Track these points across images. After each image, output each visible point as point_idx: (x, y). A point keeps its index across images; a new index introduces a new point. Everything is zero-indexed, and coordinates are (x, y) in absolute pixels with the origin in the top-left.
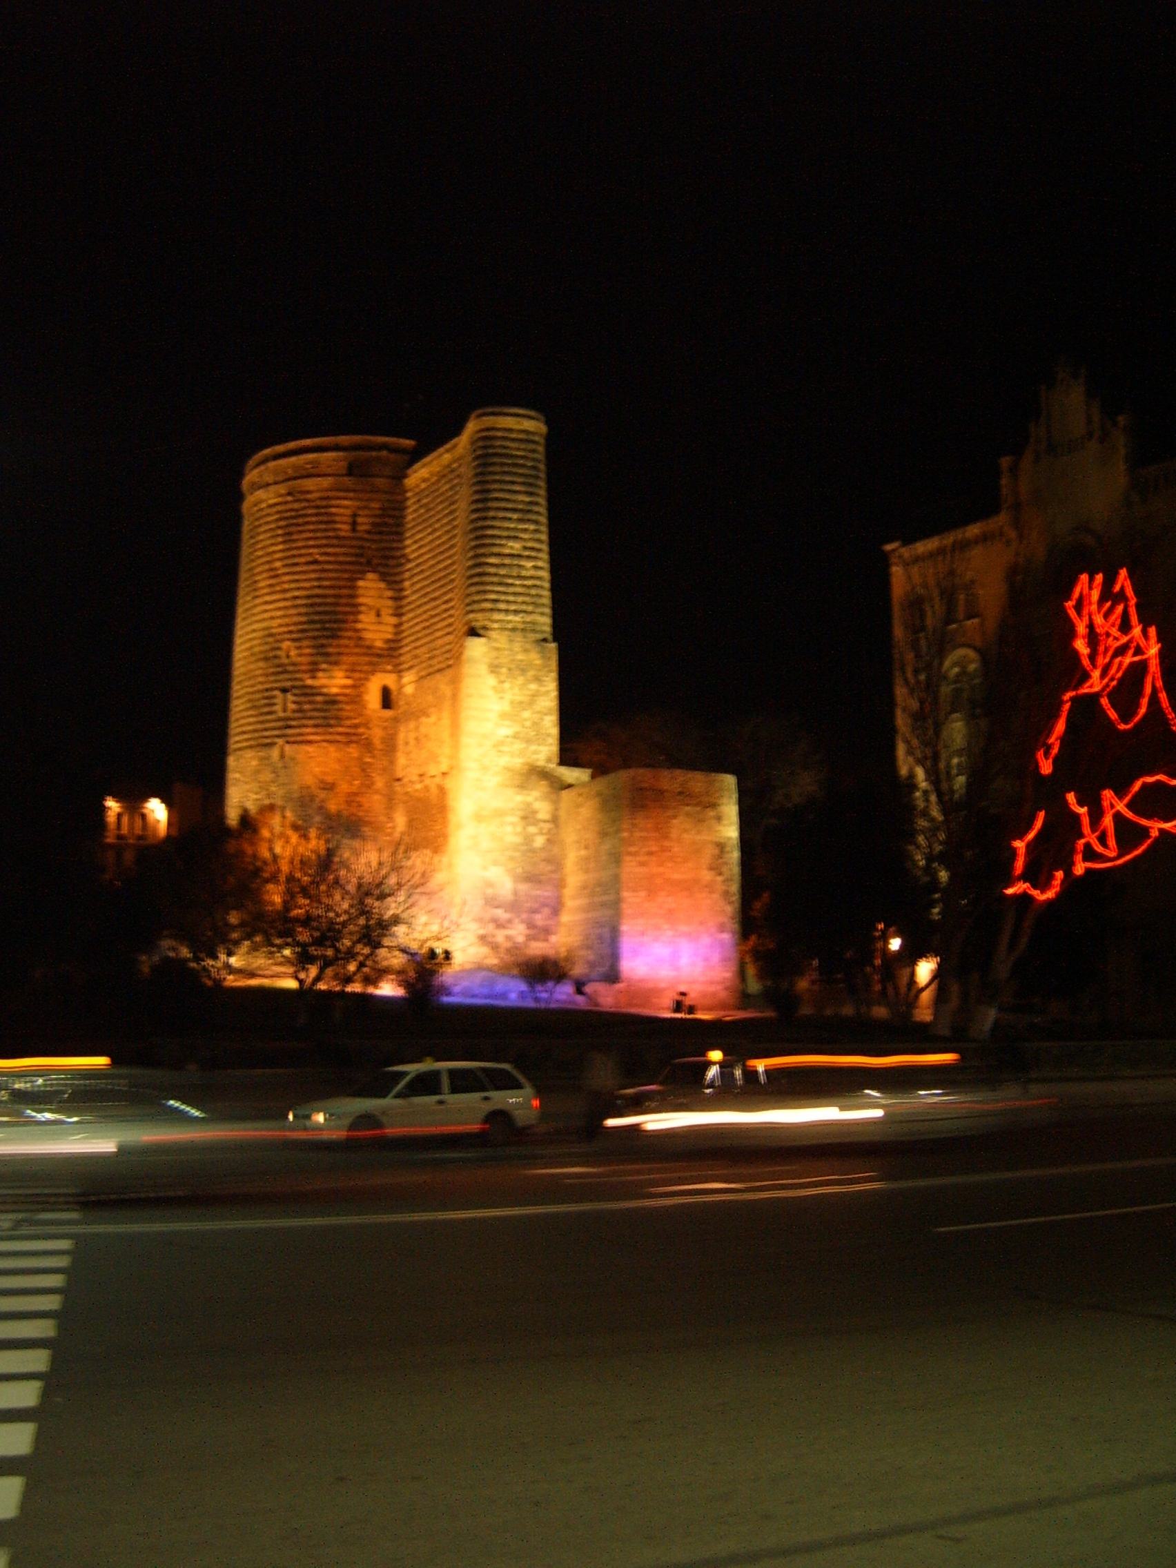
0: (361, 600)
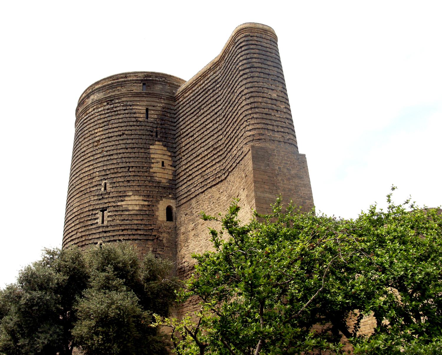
0: (152, 156)
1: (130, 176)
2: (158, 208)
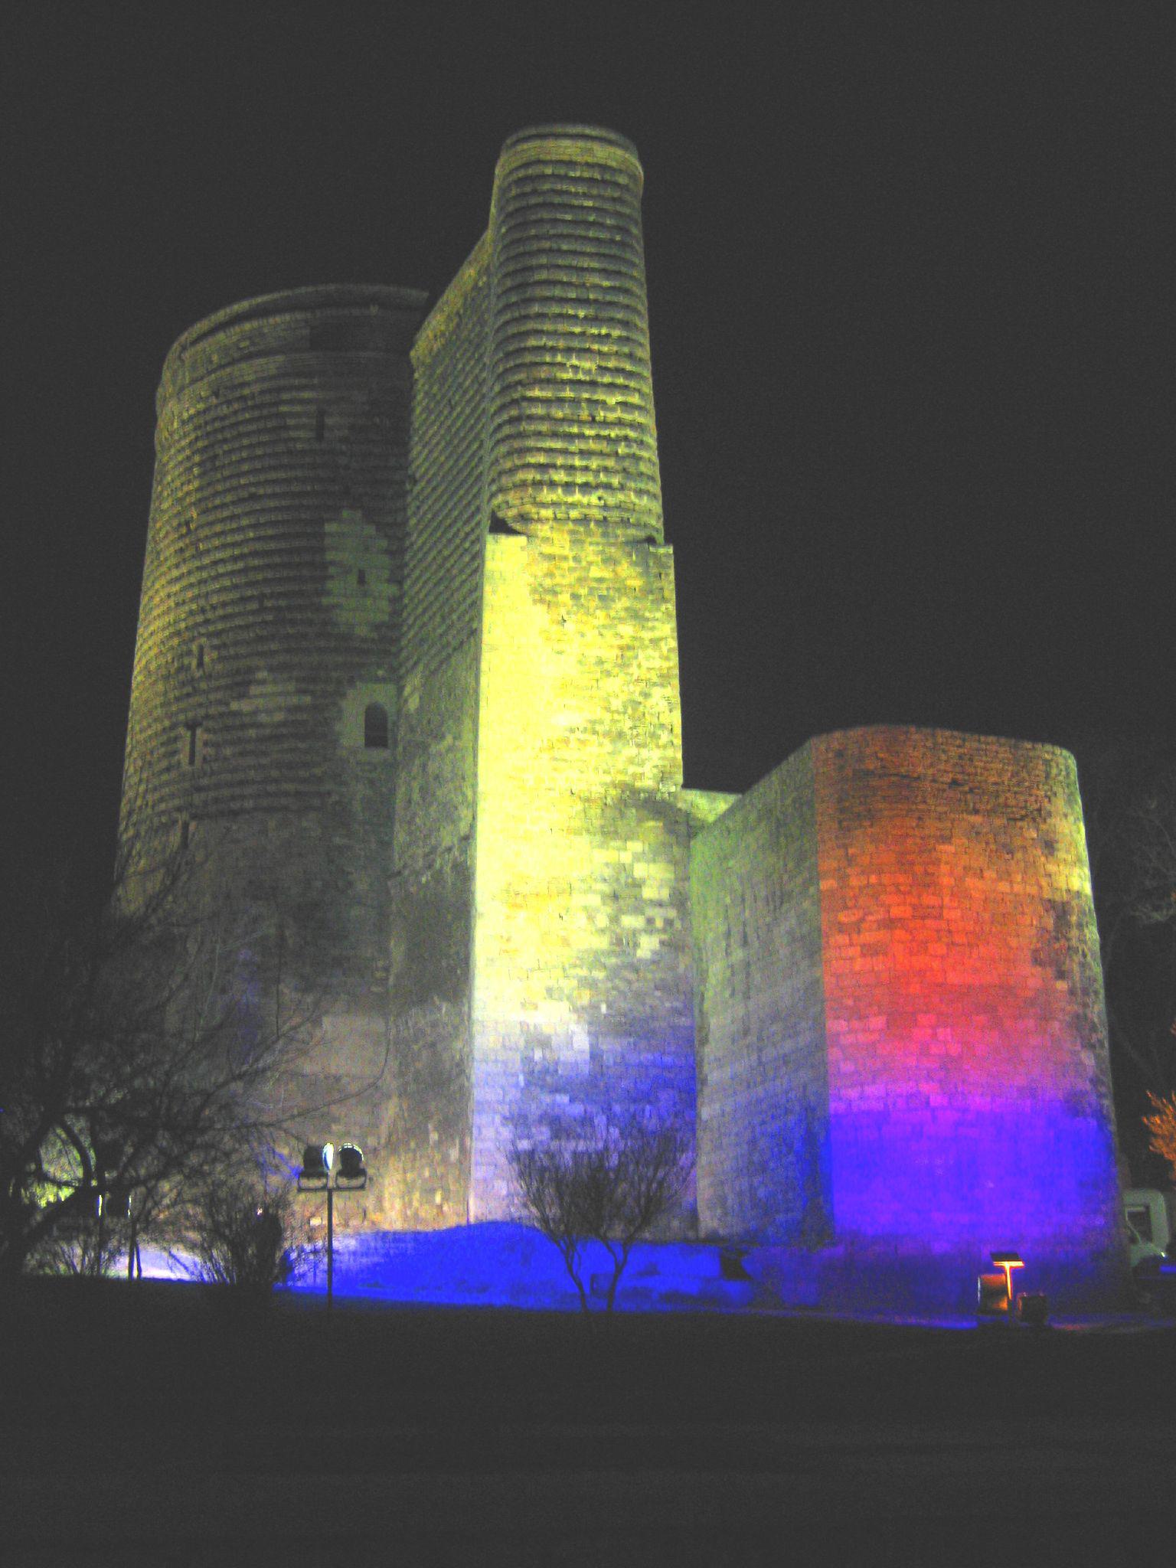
0: (330, 556)
2: (340, 711)
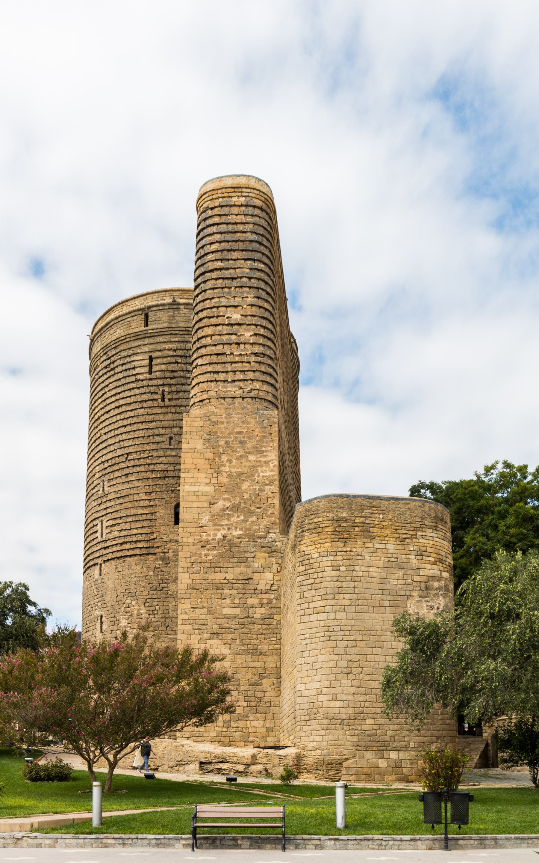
1: (128, 467)
